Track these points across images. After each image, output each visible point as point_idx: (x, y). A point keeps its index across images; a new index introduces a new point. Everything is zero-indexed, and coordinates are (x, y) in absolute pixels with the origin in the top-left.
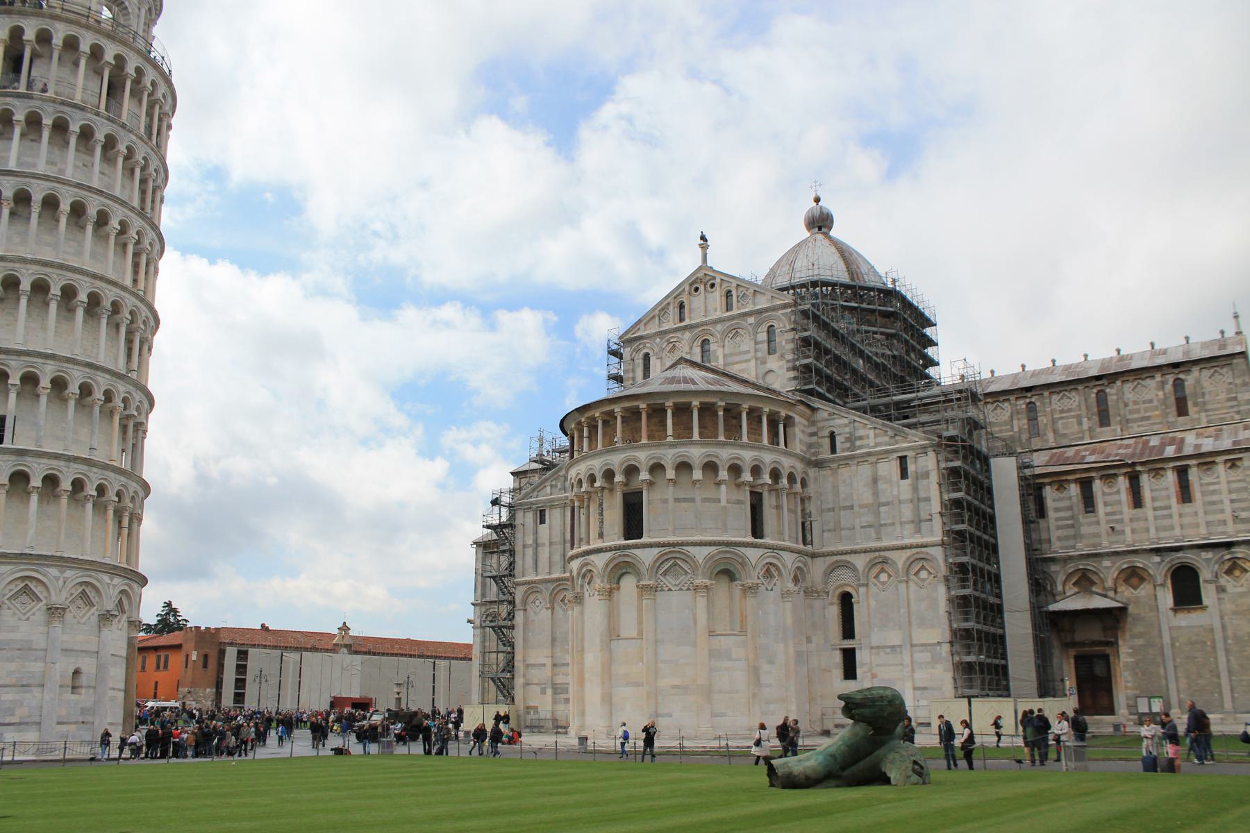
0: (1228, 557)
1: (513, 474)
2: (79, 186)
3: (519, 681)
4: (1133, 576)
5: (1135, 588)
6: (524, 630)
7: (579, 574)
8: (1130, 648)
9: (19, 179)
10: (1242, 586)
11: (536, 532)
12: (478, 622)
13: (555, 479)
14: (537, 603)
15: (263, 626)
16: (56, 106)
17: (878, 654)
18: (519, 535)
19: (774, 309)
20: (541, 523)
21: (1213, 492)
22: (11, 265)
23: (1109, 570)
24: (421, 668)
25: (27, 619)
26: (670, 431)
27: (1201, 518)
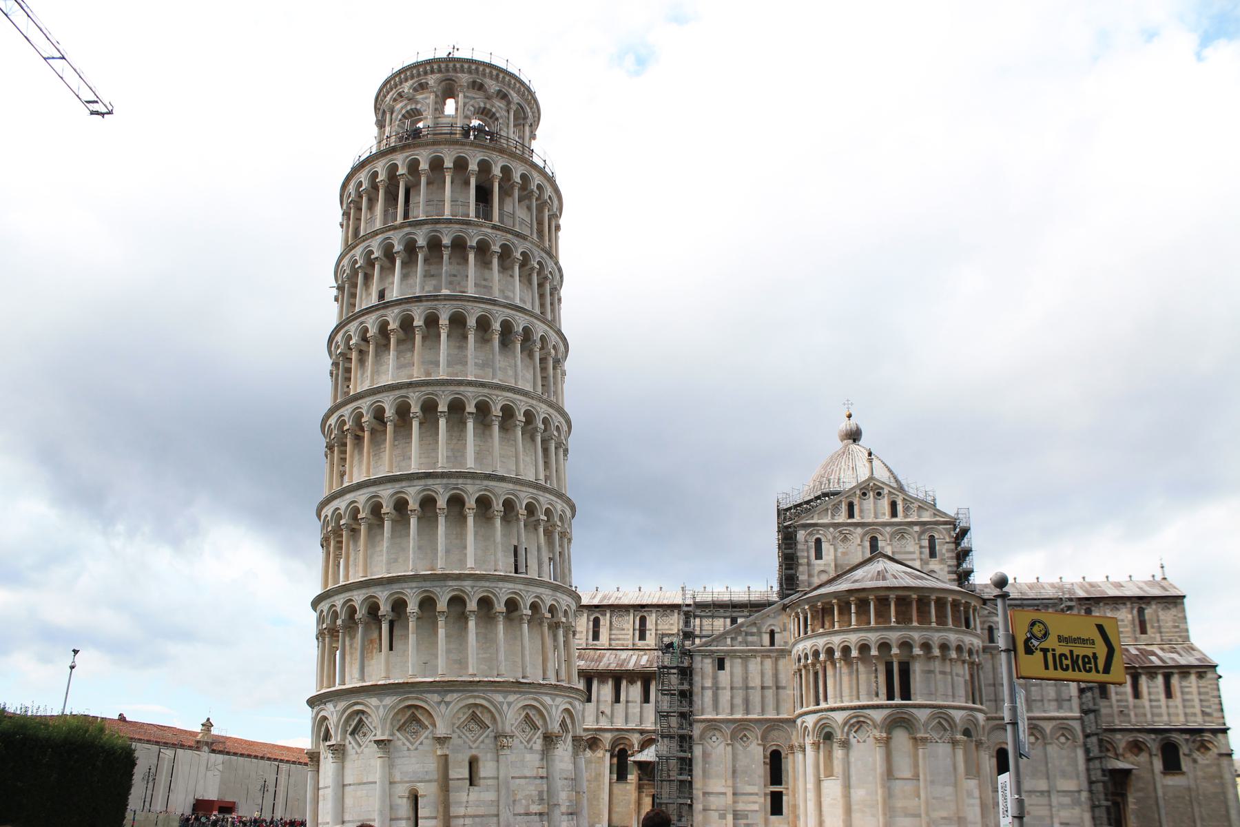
0: (1199, 739)
3: (698, 807)
4: (1137, 747)
5: (1137, 755)
7: (845, 724)
8: (1134, 799)
10: (1207, 759)
11: (715, 678)
14: (714, 738)
16: (539, 250)
17: (1030, 796)
18: (697, 679)
19: (937, 523)
20: (719, 670)
21: (1188, 693)
22: (530, 401)
23: (1121, 741)
24: (267, 768)
26: (934, 619)
27: (1180, 711)
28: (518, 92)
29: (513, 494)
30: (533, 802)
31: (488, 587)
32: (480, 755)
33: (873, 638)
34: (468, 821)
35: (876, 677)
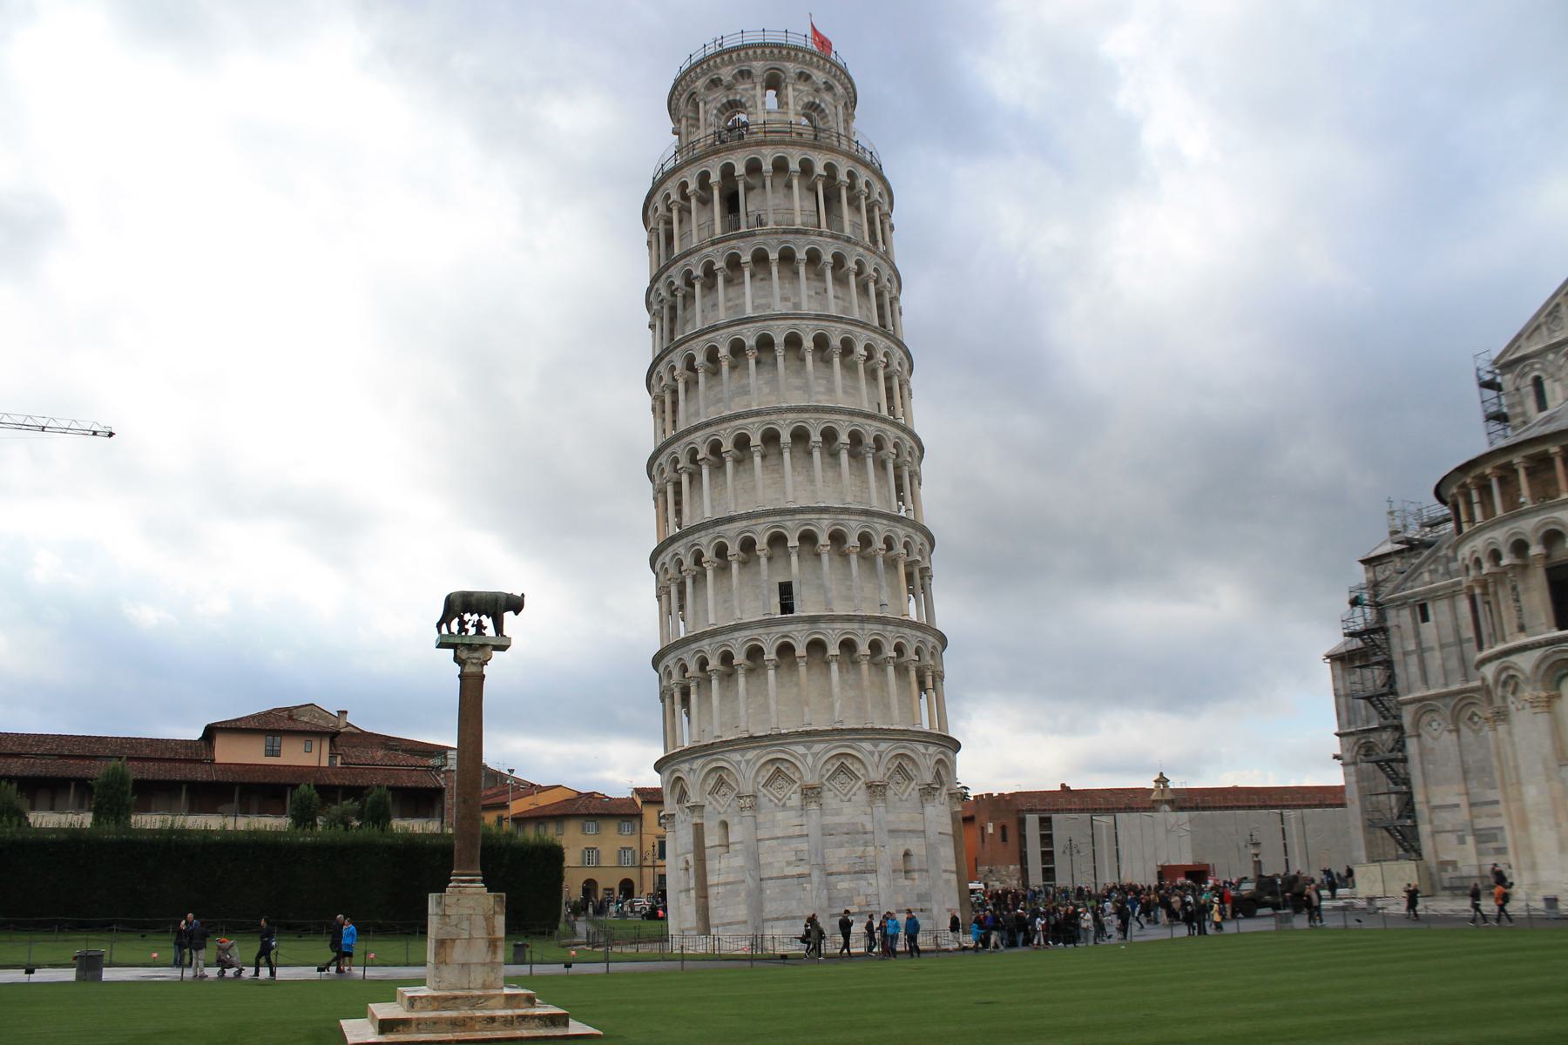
1: (1363, 562)
2: (818, 317)
3: (1424, 829)
6: (1422, 763)
7: (1496, 681)
9: (759, 324)
11: (1417, 634)
12: (1348, 757)
13: (1434, 561)
14: (1435, 724)
15: (1063, 786)
16: (779, 236)
18: (1395, 641)
22: (767, 418)
24: (1263, 821)
25: (849, 800)
28: (764, 57)
29: (748, 531)
30: (789, 864)
31: (724, 641)
32: (728, 820)
33: (1500, 536)
34: (721, 889)
35: (1517, 600)
